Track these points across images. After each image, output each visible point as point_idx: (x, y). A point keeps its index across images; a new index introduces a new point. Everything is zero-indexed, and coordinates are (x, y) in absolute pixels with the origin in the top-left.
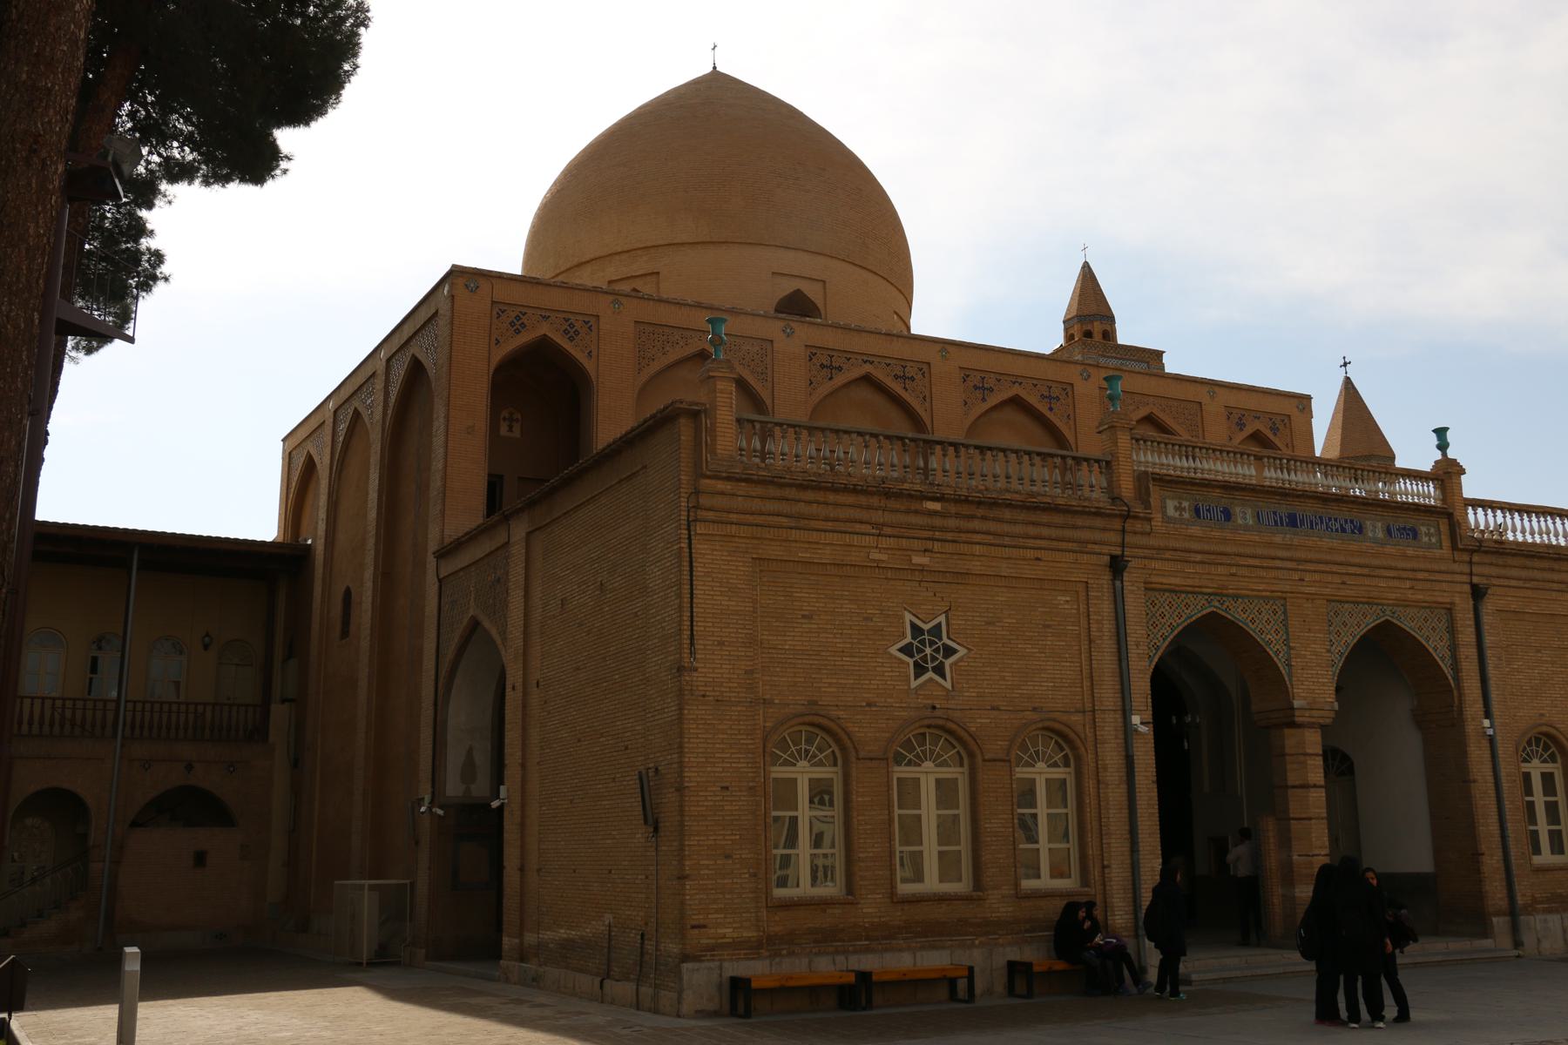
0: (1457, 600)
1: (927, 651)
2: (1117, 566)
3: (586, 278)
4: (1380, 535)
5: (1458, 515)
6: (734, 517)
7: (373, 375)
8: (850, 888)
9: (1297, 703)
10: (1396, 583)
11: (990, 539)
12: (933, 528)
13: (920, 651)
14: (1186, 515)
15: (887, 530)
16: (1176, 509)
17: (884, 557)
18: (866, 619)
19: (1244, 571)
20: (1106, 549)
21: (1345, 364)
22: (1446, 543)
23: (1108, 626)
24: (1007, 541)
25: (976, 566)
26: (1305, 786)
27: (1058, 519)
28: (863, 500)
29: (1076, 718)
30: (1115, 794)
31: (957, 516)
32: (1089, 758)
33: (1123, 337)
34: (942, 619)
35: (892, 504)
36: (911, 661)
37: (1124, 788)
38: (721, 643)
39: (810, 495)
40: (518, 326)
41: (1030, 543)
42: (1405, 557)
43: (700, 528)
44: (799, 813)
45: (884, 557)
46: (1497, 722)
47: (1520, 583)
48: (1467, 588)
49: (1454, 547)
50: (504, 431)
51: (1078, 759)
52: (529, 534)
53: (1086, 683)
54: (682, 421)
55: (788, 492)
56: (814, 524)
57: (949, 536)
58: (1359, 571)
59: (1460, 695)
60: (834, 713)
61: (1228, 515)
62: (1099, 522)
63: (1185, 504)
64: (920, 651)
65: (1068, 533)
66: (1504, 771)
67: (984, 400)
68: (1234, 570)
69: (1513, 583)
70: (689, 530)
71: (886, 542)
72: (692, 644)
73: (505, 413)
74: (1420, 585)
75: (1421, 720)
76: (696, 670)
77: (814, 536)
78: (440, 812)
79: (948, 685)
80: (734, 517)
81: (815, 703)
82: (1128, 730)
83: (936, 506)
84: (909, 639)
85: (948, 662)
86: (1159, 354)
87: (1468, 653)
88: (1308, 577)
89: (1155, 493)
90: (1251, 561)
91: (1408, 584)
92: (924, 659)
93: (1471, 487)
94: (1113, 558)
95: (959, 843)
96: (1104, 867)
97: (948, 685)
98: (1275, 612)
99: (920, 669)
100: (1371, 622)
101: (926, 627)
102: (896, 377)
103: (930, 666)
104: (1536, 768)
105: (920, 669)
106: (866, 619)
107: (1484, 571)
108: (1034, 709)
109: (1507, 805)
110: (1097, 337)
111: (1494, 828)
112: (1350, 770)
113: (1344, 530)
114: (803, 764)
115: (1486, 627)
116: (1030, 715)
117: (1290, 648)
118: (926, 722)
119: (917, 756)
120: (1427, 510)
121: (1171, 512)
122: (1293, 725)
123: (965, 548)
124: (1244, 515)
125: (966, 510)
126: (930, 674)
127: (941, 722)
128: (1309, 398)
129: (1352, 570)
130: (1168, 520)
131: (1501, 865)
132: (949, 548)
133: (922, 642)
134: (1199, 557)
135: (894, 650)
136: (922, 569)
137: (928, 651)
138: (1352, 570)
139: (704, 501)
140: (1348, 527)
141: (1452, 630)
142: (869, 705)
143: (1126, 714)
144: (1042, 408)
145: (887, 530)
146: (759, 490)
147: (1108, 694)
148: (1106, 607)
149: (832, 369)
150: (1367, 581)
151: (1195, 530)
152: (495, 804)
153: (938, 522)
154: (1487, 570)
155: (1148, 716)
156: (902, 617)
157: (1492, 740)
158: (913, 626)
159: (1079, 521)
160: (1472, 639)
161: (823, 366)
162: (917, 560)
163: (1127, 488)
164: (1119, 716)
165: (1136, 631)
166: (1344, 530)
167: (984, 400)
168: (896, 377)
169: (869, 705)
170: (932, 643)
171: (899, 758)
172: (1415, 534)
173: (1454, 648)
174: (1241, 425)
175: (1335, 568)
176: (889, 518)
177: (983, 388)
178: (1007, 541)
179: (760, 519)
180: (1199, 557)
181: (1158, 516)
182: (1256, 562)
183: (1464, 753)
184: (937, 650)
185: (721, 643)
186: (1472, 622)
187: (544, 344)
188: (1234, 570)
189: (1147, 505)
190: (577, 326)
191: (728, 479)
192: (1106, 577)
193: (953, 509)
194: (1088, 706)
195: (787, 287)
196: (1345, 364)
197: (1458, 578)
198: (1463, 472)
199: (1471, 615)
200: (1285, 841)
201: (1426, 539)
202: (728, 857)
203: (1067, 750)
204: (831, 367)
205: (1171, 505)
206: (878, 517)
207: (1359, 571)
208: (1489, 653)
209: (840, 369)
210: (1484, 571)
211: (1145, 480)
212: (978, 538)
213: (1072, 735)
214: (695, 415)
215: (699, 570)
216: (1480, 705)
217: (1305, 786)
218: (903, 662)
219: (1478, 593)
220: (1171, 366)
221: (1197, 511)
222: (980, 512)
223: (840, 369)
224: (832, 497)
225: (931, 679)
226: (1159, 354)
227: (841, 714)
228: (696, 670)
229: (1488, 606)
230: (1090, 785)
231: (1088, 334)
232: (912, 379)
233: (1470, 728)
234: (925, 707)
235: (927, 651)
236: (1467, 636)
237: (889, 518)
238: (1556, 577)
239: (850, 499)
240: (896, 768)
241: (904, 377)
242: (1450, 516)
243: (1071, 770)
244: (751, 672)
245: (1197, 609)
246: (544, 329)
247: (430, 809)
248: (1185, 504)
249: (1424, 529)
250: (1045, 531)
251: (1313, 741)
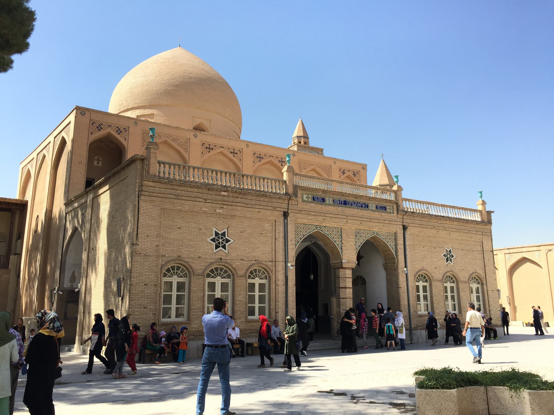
0: (398, 230)
1: (220, 240)
2: (286, 215)
3: (129, 114)
4: (374, 209)
5: (400, 203)
6: (155, 194)
7: (50, 143)
8: (189, 319)
9: (343, 261)
10: (378, 224)
11: (243, 205)
12: (224, 201)
13: (217, 240)
14: (310, 200)
15: (208, 201)
16: (307, 197)
17: (207, 210)
18: (200, 229)
19: (328, 218)
20: (282, 210)
21: (382, 155)
22: (395, 212)
23: (282, 235)
24: (249, 206)
25: (238, 213)
26: (345, 288)
27: (267, 200)
28: (200, 190)
29: (270, 263)
30: (281, 289)
31: (233, 197)
32: (273, 277)
33: (312, 144)
34: (226, 230)
35: (210, 192)
36: (214, 244)
37: (284, 287)
38: (148, 236)
39: (182, 188)
40: (100, 128)
41: (257, 207)
42: (381, 215)
43: (142, 198)
44: (172, 293)
45: (207, 210)
46: (409, 269)
47: (419, 226)
48: (402, 227)
49: (398, 213)
50: (95, 163)
51: (270, 277)
52: (93, 198)
53: (274, 253)
54: (138, 161)
55: (174, 187)
56: (183, 198)
57: (229, 203)
58: (366, 220)
59: (397, 260)
60: (186, 260)
61: (324, 200)
62: (280, 201)
63: (310, 196)
64: (217, 240)
65: (270, 204)
66: (410, 284)
67: (260, 161)
68: (325, 218)
69: (416, 225)
70: (138, 198)
71: (207, 205)
72: (137, 236)
73: (96, 158)
74: (386, 225)
75: (386, 268)
76: (138, 245)
77: (183, 202)
78: (61, 293)
79: (227, 252)
80: (155, 194)
81: (180, 256)
82: (286, 267)
83: (226, 194)
84: (214, 236)
85: (227, 244)
86: (322, 150)
87: (401, 247)
88: (349, 221)
89: (300, 193)
90: (330, 215)
91: (382, 224)
92: (219, 243)
93: (405, 194)
94: (284, 212)
95: (184, 304)
96: (276, 312)
97: (227, 252)
98: (338, 232)
99: (217, 247)
100: (368, 237)
101: (220, 233)
102: (231, 152)
103: (221, 245)
104: (421, 284)
105: (217, 247)
106: (200, 229)
107: (407, 221)
108: (256, 260)
109: (411, 295)
110: (302, 143)
111: (406, 303)
112: (365, 283)
113: (362, 207)
114: (175, 277)
115: (407, 239)
116: (254, 262)
117: (342, 243)
118: (218, 264)
119: (215, 275)
120: (390, 201)
121: (305, 198)
122: (342, 268)
123: (235, 207)
125: (235, 195)
126: (221, 248)
127: (223, 264)
128: (366, 165)
129: (364, 219)
130: (303, 201)
131: (408, 315)
132: (230, 207)
133: (219, 238)
134: (313, 213)
135: (209, 240)
136: (220, 214)
137: (220, 240)
138: (364, 219)
139: (144, 188)
140: (363, 206)
141: (396, 240)
142: (199, 257)
143: (286, 262)
145: (208, 201)
146: (164, 186)
147: (280, 257)
148: (281, 228)
149: (210, 149)
150: (369, 223)
151: (312, 205)
152: (76, 290)
153: (226, 198)
154: (409, 221)
155: (294, 263)
156: (212, 229)
157: (407, 275)
158: (216, 232)
159: (274, 201)
160: (402, 242)
161: (206, 148)
162: (218, 211)
163: (291, 191)
164: (284, 263)
166: (362, 207)
167: (260, 161)
168: (231, 152)
169: (199, 257)
170: (222, 238)
171: (208, 276)
172: (385, 208)
173: (396, 245)
174: (344, 173)
175: (358, 219)
176: (209, 197)
177: (260, 158)
178: (249, 206)
179: (163, 196)
180: (313, 213)
181: (300, 200)
182: (332, 216)
183: (398, 279)
184: (223, 240)
185: (148, 236)
186: (402, 237)
187: (109, 134)
188: (325, 218)
189: (296, 196)
190: (121, 130)
191: (153, 182)
192: (282, 218)
193: (231, 195)
194: (274, 260)
195: (197, 122)
196: (382, 155)
197: (399, 223)
198: (402, 189)
199: (402, 235)
200: (339, 305)
201: (389, 210)
202: (145, 308)
203: (266, 274)
204: (209, 148)
205: (305, 196)
206: (205, 196)
207: (366, 220)
208: (407, 247)
209: (212, 149)
210: (407, 221)
211: (296, 187)
212: (239, 204)
213: (268, 269)
214: (142, 160)
215: (141, 211)
216: (404, 264)
217: (345, 288)
218: (211, 244)
219: (405, 228)
220: (326, 154)
221: (314, 198)
222: (240, 196)
223: (212, 149)
224: (190, 189)
225: (221, 250)
226: (322, 150)
227: (189, 260)
228: (138, 245)
229: (408, 233)
230: (273, 285)
231: (300, 142)
232: (237, 153)
233: (400, 271)
234: (218, 258)
235: (220, 240)
236: (400, 242)
237: (209, 197)
238: (430, 224)
239: (196, 190)
240: (208, 279)
241: (234, 153)
242: (397, 204)
243: (267, 280)
244: (158, 246)
245: (312, 230)
246: (109, 130)
247: (57, 292)
248: (310, 196)
249: (388, 207)
250: (262, 203)
251: (349, 273)
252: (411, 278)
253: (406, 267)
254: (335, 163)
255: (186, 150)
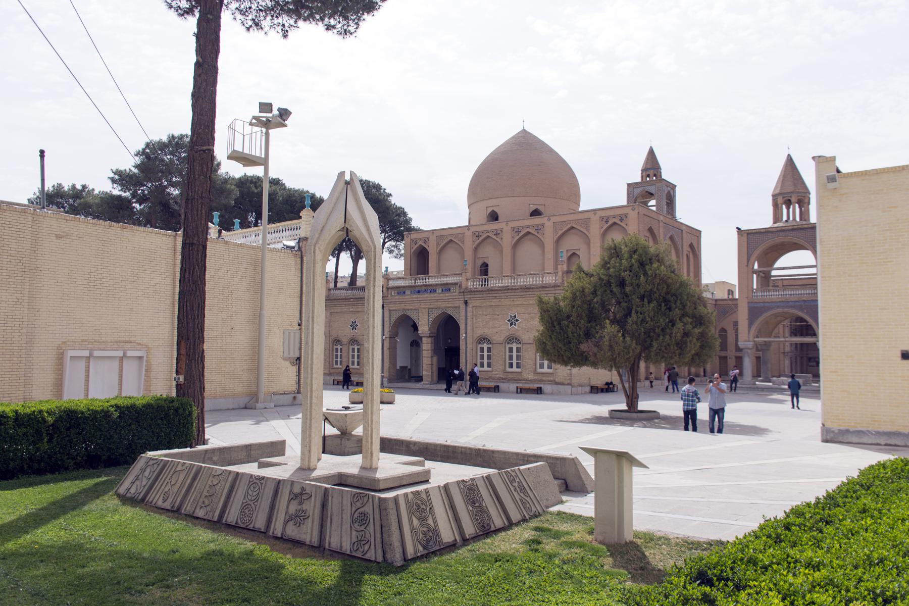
1: (354, 326)
40: (416, 243)
107: (467, 297)
124: (408, 292)
144: (535, 233)
165: (386, 319)
174: (607, 222)
195: (490, 210)
210: (467, 297)
219: (466, 303)
236: (463, 314)
245: (401, 313)
246: (421, 243)
252: (469, 342)
253: (466, 333)
254: (595, 214)
255: (463, 242)
